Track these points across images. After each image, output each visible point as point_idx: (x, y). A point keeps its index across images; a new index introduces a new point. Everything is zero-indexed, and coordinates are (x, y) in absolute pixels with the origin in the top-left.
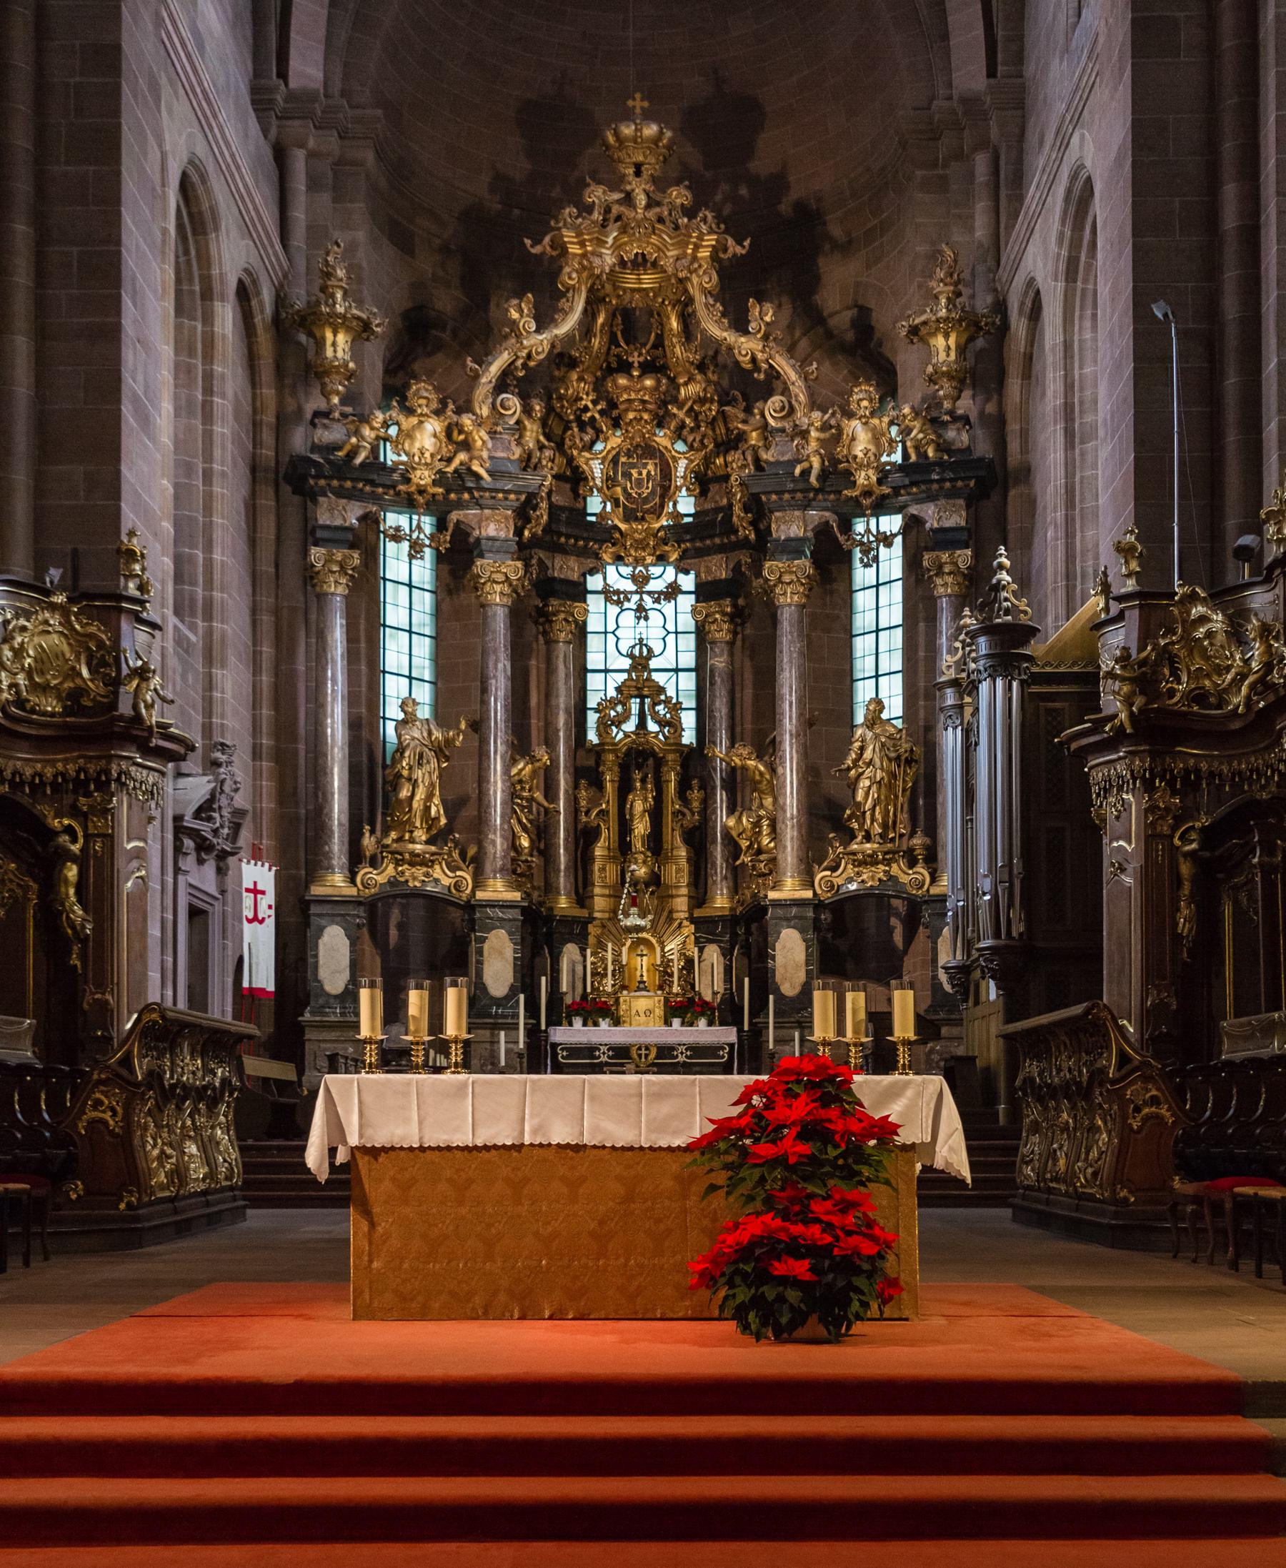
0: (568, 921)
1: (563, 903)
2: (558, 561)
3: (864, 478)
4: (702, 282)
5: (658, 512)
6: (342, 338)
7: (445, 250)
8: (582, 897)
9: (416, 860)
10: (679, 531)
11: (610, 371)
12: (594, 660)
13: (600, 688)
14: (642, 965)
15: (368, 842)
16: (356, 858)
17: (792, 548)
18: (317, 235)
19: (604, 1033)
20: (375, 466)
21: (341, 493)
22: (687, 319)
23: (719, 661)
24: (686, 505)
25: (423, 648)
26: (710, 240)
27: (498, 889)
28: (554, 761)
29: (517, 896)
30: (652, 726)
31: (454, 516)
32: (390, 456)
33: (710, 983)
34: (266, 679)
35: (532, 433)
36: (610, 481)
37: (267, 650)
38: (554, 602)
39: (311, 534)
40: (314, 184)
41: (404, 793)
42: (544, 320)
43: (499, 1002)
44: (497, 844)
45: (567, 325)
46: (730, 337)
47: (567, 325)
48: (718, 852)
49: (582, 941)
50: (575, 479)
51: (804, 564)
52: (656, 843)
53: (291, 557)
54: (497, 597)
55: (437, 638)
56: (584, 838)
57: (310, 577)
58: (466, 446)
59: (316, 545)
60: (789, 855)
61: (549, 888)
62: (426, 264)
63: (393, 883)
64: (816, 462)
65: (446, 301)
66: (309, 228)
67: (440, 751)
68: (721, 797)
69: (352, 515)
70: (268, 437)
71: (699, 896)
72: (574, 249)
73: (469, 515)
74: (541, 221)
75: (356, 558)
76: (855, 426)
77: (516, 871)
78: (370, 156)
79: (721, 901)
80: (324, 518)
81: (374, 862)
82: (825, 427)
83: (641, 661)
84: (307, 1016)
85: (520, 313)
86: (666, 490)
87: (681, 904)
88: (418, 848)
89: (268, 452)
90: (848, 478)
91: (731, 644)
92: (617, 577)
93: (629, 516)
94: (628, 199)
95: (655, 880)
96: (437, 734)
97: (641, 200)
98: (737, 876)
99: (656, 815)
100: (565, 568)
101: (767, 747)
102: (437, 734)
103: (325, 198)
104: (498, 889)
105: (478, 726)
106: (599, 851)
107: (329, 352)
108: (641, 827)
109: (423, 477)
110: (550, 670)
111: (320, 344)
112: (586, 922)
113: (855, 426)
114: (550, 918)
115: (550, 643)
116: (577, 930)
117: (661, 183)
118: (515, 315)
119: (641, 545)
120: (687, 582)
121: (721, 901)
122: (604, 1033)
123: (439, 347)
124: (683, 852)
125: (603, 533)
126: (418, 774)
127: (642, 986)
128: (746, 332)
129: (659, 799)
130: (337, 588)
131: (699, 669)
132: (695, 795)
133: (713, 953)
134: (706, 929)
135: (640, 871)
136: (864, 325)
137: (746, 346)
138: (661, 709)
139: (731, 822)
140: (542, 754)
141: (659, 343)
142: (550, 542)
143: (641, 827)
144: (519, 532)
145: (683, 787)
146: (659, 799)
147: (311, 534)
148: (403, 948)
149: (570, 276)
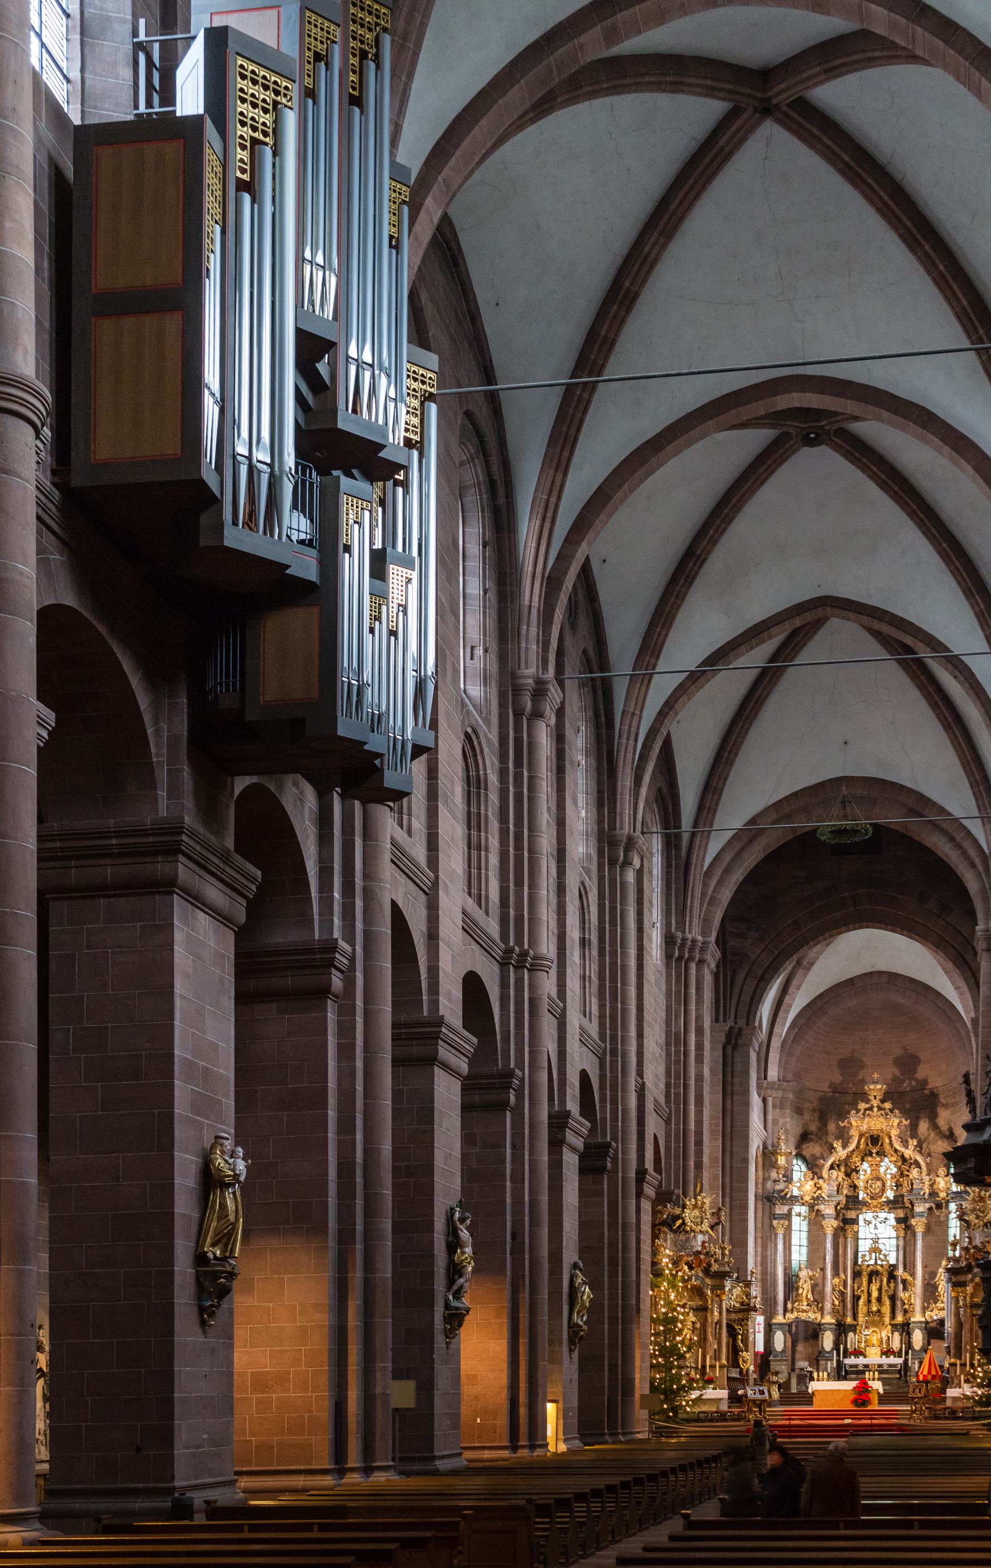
0: (850, 1326)
1: (849, 1320)
2: (849, 1212)
3: (942, 1195)
4: (894, 1133)
5: (881, 1197)
6: (783, 1158)
7: (814, 1110)
8: (855, 1317)
9: (804, 1311)
10: (889, 1202)
11: (866, 1155)
12: (861, 1235)
13: (864, 1246)
14: (874, 1339)
15: (789, 1306)
16: (785, 1310)
17: (921, 1214)
18: (775, 1122)
19: (861, 1361)
20: (792, 1196)
21: (782, 1204)
22: (890, 1137)
23: (901, 1243)
24: (890, 1194)
25: (804, 1235)
26: (896, 1121)
27: (828, 1319)
28: (846, 1276)
29: (834, 1321)
30: (879, 1262)
31: (816, 1207)
32: (796, 1192)
33: (896, 1344)
34: (759, 1258)
35: (841, 1175)
36: (866, 1188)
37: (759, 1250)
38: (847, 1226)
39: (773, 1216)
40: (774, 1106)
41: (800, 1291)
42: (844, 1146)
43: (828, 1353)
44: (828, 1306)
45: (852, 1147)
46: (903, 1149)
47: (852, 1147)
48: (899, 1304)
49: (855, 1331)
50: (854, 1187)
51: (924, 1220)
52: (879, 1300)
53: (767, 1221)
54: (829, 1232)
55: (809, 1232)
56: (856, 1298)
57: (772, 1226)
58: (820, 1188)
59: (775, 1219)
60: (918, 1307)
61: (844, 1315)
62: (807, 1116)
63: (797, 1318)
64: (927, 1191)
65: (813, 1127)
66: (773, 1120)
67: (811, 1278)
68: (901, 1286)
69: (785, 1209)
70: (760, 1186)
71: (893, 1316)
72: (854, 1124)
73: (822, 1207)
74: (843, 1115)
75: (787, 1223)
76: (939, 1179)
77: (834, 1312)
78: (791, 1096)
79: (900, 1319)
80: (777, 1212)
81: (792, 1311)
82: (930, 1180)
83: (875, 1241)
84: (771, 1358)
85: (837, 1145)
86: (883, 1190)
87: (887, 1320)
88: (804, 1308)
89: (760, 1191)
90: (937, 1194)
91: (904, 1237)
92: (869, 1216)
93: (872, 1198)
94: (871, 1109)
95: (879, 1311)
96: (811, 1273)
97: (875, 1109)
98: (906, 1311)
99: (880, 1290)
100: (851, 1214)
101: (913, 1275)
102: (811, 1273)
103: (778, 1110)
104: (828, 1319)
105: (823, 1270)
106: (861, 1302)
107: (779, 1162)
108: (875, 1294)
109: (807, 1198)
110: (845, 1247)
111: (777, 1160)
112: (855, 1326)
113: (939, 1179)
114: (844, 1325)
115: (846, 1238)
116: (853, 1328)
117: (883, 1101)
118: (835, 1145)
119: (876, 1207)
120: (892, 1216)
121: (900, 1319)
122: (861, 1361)
123: (811, 1140)
124: (887, 1302)
125: (864, 1203)
126: (805, 1286)
127: (873, 1345)
128: (907, 1148)
129: (881, 1286)
130: (781, 1232)
131: (897, 1238)
132: (892, 1285)
133: (897, 1335)
134: (894, 1327)
135: (874, 1309)
136: (950, 1130)
137: (909, 1153)
138: (882, 1257)
139: (902, 1295)
140: (843, 1276)
141: (882, 1145)
142: (847, 1208)
143: (875, 1294)
144: (836, 1207)
145: (889, 1282)
146: (881, 1286)
147: (773, 1216)
148: (797, 1333)
149: (854, 1133)
